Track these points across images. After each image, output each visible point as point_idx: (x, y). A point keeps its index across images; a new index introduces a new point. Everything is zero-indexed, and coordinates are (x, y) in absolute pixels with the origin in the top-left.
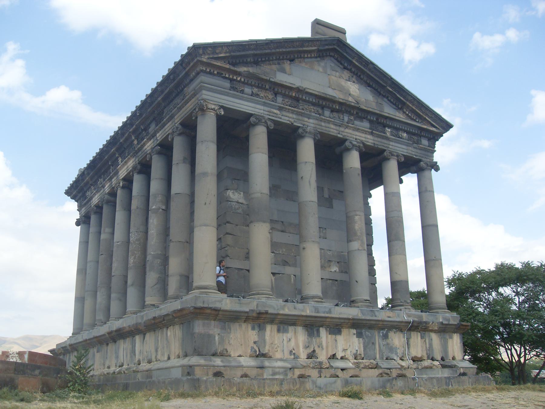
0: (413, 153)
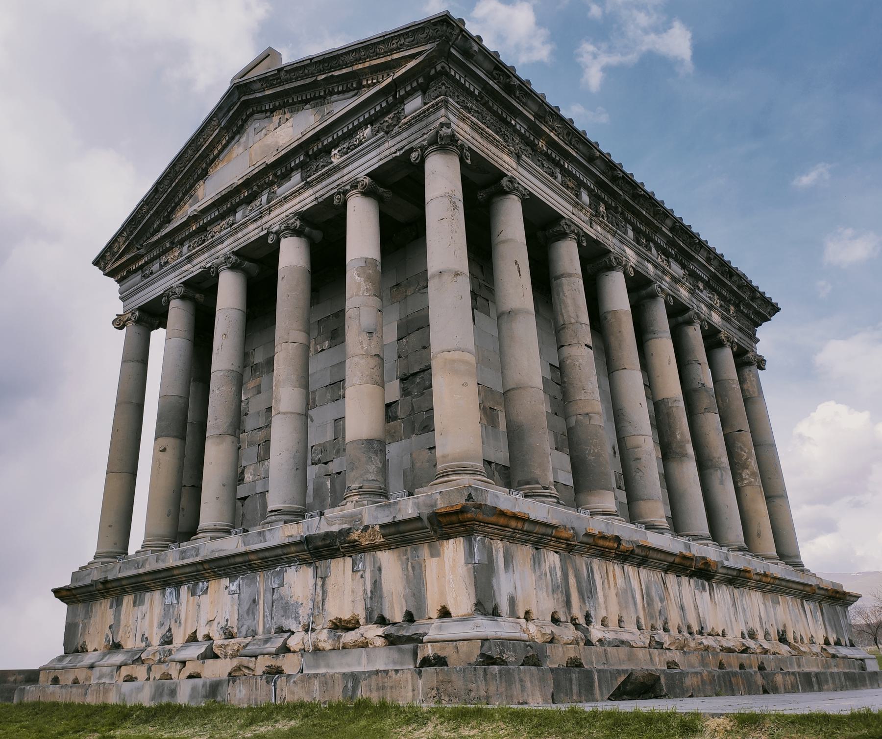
0: (393, 150)
